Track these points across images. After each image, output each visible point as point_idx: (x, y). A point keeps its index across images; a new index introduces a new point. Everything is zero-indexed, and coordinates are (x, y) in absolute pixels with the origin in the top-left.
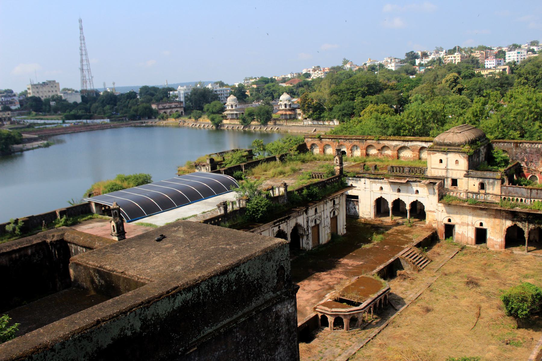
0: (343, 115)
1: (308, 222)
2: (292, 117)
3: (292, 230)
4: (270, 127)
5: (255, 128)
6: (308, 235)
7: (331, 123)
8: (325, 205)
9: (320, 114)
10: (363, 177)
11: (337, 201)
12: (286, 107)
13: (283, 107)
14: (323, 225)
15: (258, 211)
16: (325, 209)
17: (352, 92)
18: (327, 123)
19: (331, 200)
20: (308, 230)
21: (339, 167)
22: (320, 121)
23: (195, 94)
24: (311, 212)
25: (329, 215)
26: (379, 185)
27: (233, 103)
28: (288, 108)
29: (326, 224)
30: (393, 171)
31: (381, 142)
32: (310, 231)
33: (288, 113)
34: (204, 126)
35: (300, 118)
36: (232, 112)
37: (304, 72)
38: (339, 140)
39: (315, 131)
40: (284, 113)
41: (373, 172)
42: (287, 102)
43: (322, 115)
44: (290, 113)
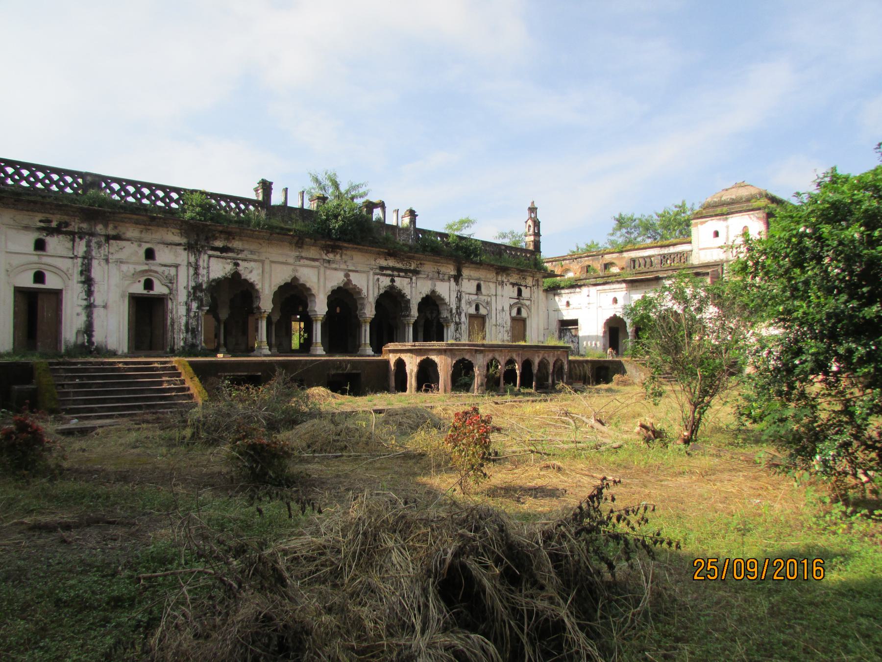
1: (459, 299)
3: (423, 299)
6: (458, 324)
8: (499, 287)
10: (584, 285)
11: (526, 293)
14: (493, 321)
15: (336, 216)
16: (499, 293)
19: (513, 285)
20: (459, 314)
21: (532, 238)
24: (468, 286)
25: (507, 308)
26: (612, 295)
29: (499, 321)
30: (634, 267)
31: (625, 255)
32: (463, 319)
38: (563, 263)
41: (601, 274)
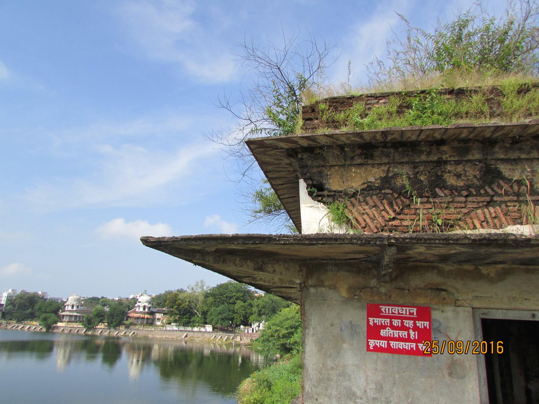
0: (222, 319)
2: (150, 321)
4: (121, 332)
5: (101, 332)
7: (203, 329)
9: (190, 318)
12: (144, 309)
13: (141, 309)
17: (227, 297)
18: (196, 329)
22: (188, 326)
23: (21, 298)
27: (75, 303)
28: (146, 310)
33: (146, 316)
34: (29, 328)
35: (158, 323)
36: (71, 314)
37: (131, 297)
39: (186, 336)
40: (142, 316)
42: (147, 304)
43: (192, 320)
44: (149, 316)
